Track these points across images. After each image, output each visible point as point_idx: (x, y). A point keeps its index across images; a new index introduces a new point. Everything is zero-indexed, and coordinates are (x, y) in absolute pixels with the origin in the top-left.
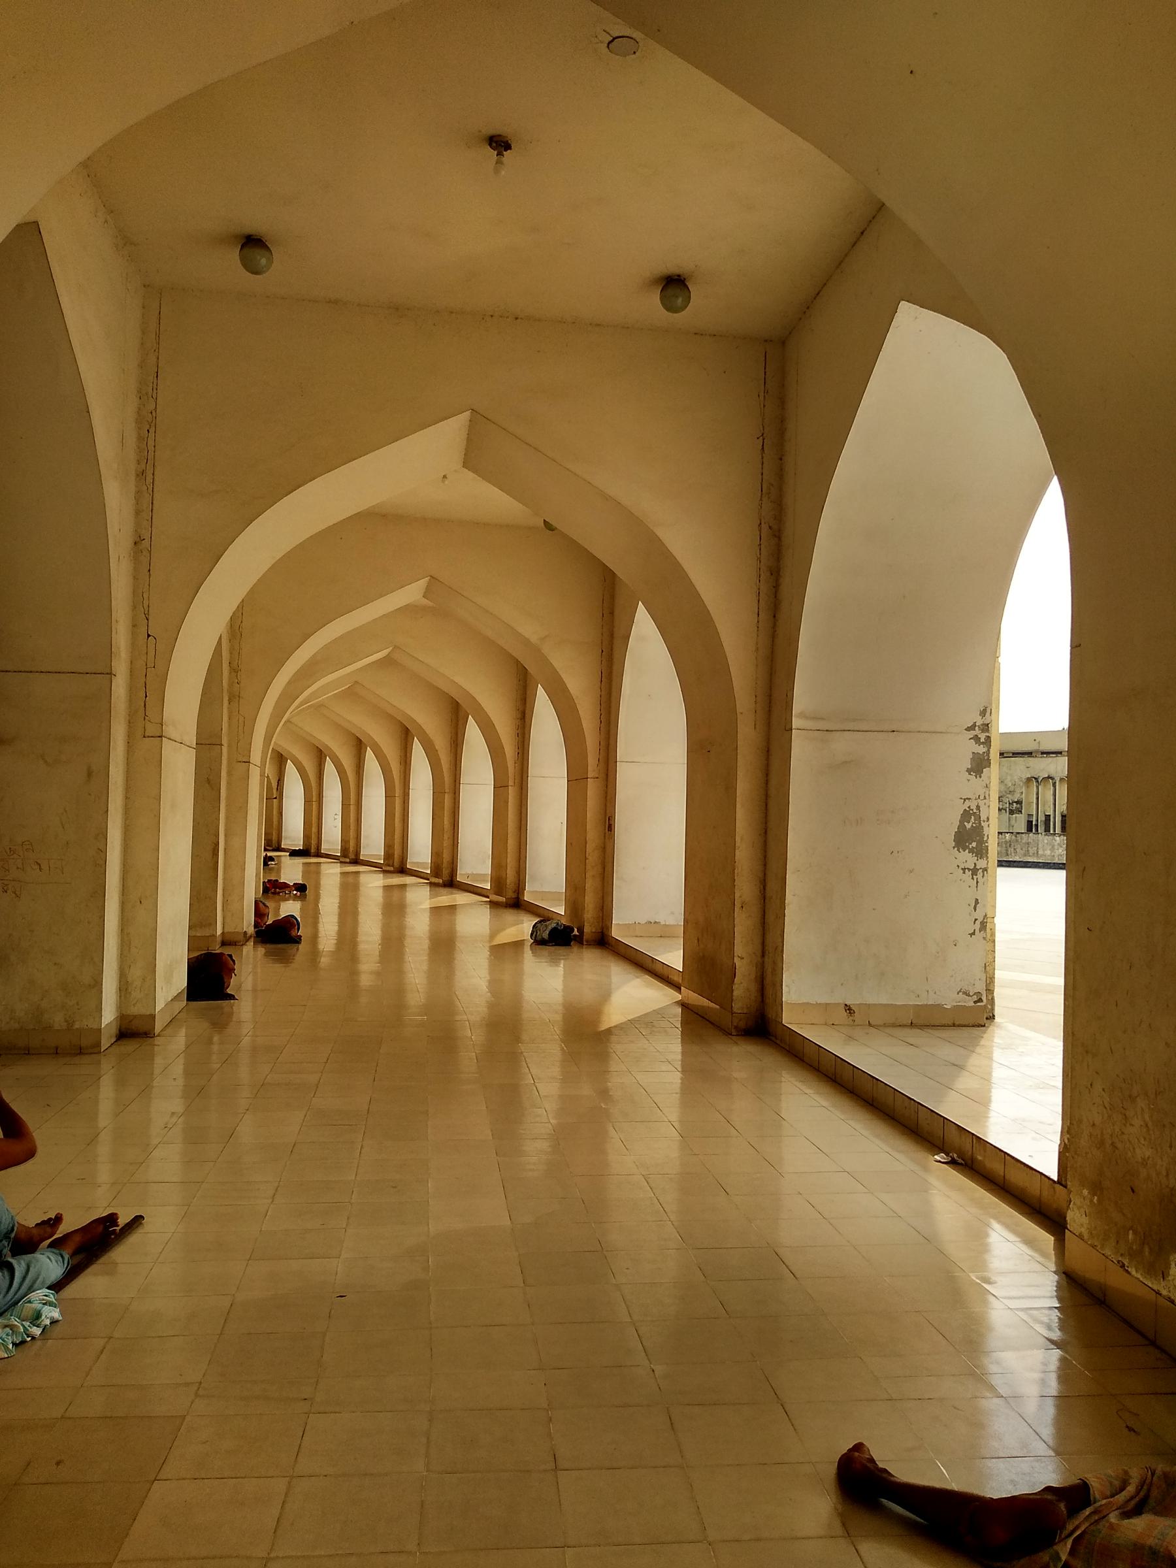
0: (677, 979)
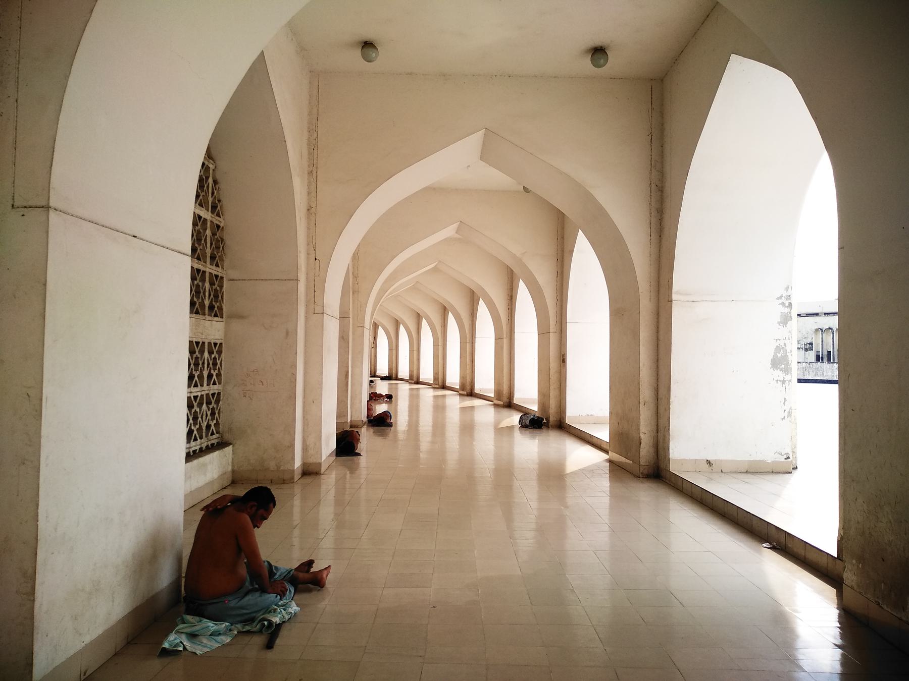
0: (606, 447)
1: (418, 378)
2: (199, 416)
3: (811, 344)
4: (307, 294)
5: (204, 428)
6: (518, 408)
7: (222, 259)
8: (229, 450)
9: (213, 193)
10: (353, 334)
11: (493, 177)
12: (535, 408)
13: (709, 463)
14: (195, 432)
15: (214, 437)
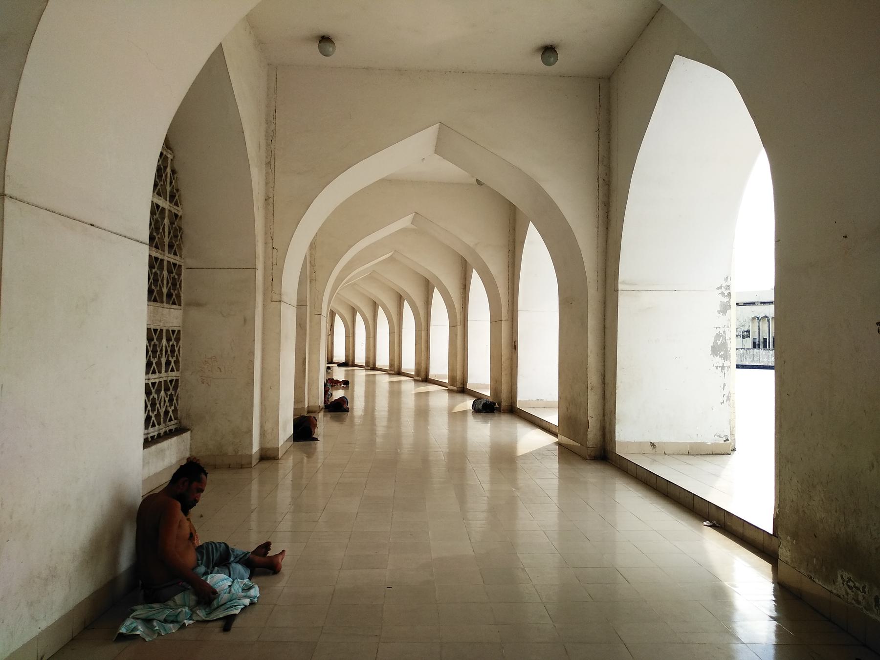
0: (555, 430)
1: (374, 364)
2: (157, 403)
3: (748, 331)
4: (264, 283)
5: (162, 414)
6: (471, 393)
7: (180, 248)
8: (187, 435)
9: (171, 183)
10: (311, 321)
11: (448, 170)
12: (487, 393)
13: (652, 445)
14: (153, 418)
15: (172, 423)
